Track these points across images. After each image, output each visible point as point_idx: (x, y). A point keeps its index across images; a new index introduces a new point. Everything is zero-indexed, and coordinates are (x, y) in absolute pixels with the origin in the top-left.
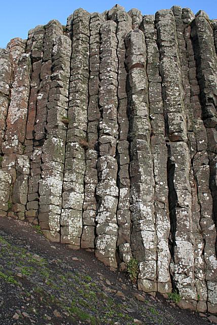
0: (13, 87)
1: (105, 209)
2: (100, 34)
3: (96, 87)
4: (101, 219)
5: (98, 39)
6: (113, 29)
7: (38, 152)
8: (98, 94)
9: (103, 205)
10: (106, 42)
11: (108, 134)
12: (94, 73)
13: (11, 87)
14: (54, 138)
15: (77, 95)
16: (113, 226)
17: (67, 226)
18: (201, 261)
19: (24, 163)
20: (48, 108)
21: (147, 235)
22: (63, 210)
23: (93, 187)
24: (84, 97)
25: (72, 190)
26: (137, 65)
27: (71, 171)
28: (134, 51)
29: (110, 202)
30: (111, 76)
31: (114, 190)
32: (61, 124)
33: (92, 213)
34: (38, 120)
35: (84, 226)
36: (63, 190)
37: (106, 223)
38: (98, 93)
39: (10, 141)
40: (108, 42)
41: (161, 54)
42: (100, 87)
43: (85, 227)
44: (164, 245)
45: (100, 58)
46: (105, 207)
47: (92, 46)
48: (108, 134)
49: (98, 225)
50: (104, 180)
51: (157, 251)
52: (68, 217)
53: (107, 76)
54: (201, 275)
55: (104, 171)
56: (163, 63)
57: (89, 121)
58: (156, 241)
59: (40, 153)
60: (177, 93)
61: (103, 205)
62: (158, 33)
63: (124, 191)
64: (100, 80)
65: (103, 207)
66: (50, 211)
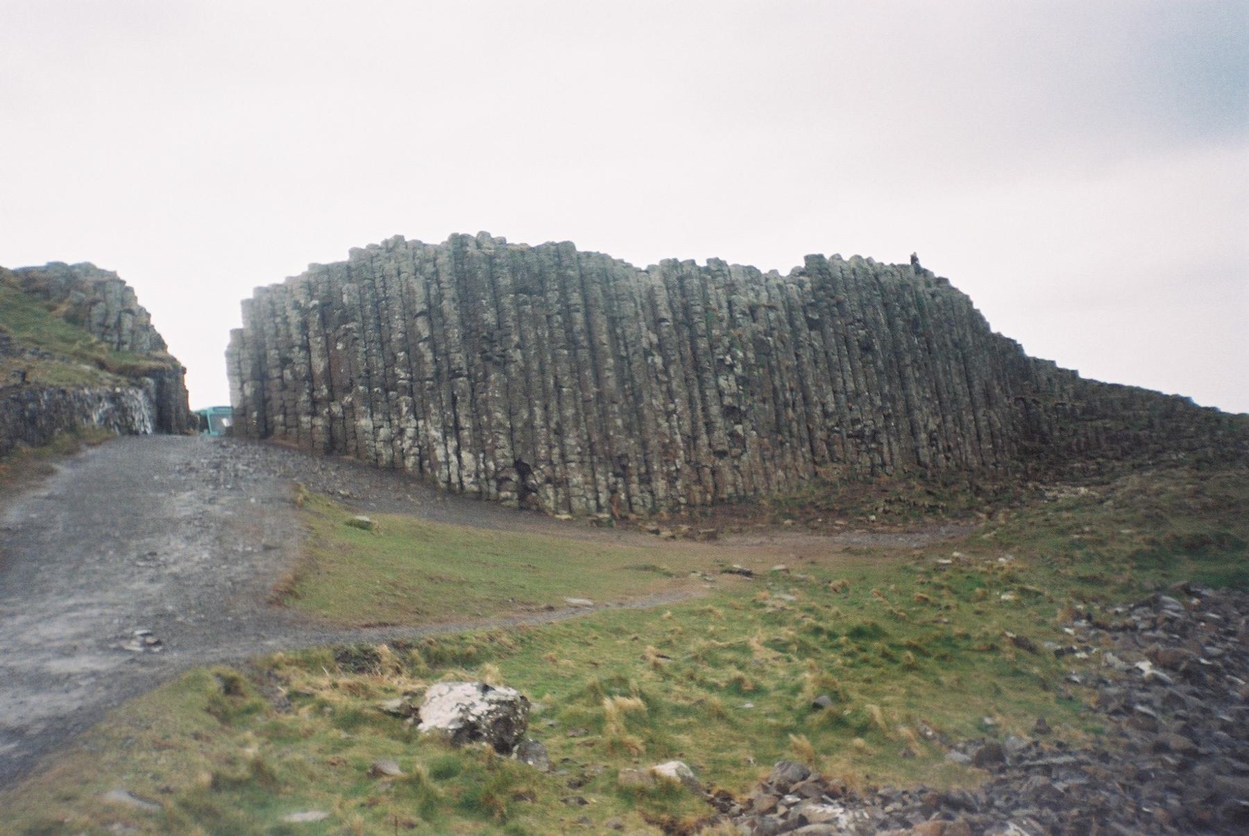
4: (406, 445)
6: (394, 272)
7: (348, 399)
12: (381, 320)
16: (416, 450)
18: (482, 466)
19: (336, 409)
21: (440, 452)
24: (379, 346)
26: (421, 313)
29: (410, 432)
31: (414, 423)
37: (410, 448)
38: (390, 340)
39: (320, 390)
41: (440, 297)
44: (454, 458)
51: (448, 463)
54: (482, 476)
58: (447, 455)
60: (455, 334)
62: (436, 273)
63: (421, 423)
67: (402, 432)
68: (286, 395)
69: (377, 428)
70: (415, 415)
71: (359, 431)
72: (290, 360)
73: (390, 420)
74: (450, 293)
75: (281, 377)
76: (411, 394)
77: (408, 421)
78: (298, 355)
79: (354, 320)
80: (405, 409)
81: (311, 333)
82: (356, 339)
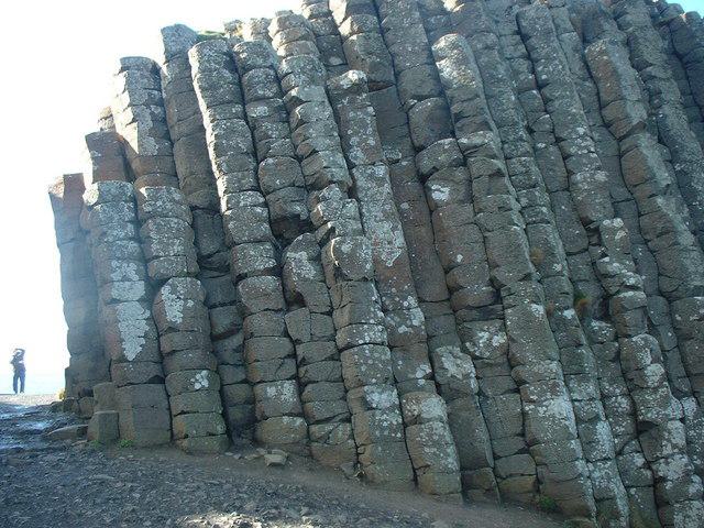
0: (354, 166)
1: (676, 450)
2: (524, 38)
3: (560, 171)
5: (522, 49)
8: (567, 189)
9: (669, 440)
10: (549, 59)
11: (633, 288)
13: (351, 166)
14: (534, 306)
15: (537, 193)
17: (613, 498)
20: (482, 229)
22: (590, 465)
23: (624, 404)
25: (597, 418)
27: (581, 375)
28: (625, 93)
30: (592, 150)
32: (532, 268)
33: (639, 461)
34: (460, 258)
35: (627, 488)
36: (578, 421)
40: (557, 62)
42: (570, 173)
43: (633, 491)
45: (546, 101)
46: (674, 446)
47: (515, 64)
48: (633, 288)
49: (669, 485)
50: (655, 390)
52: (609, 479)
53: (580, 148)
55: (649, 368)
56: (665, 116)
57: (569, 254)
59: (499, 340)
61: (669, 440)
64: (566, 157)
65: (669, 446)
66: (581, 475)
67: (644, 430)
68: (297, 320)
69: (585, 421)
70: (669, 381)
71: (543, 432)
72: (308, 226)
73: (604, 397)
74: (671, 92)
75: (279, 271)
76: (653, 329)
77: (665, 403)
78: (328, 206)
79: (485, 126)
80: (654, 371)
81: (358, 154)
82: (499, 174)
